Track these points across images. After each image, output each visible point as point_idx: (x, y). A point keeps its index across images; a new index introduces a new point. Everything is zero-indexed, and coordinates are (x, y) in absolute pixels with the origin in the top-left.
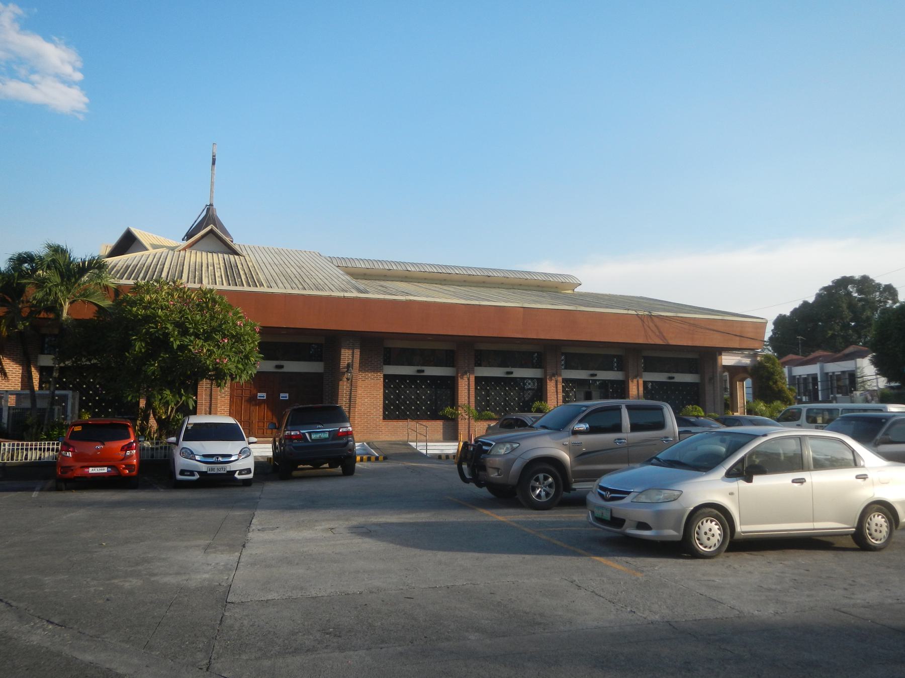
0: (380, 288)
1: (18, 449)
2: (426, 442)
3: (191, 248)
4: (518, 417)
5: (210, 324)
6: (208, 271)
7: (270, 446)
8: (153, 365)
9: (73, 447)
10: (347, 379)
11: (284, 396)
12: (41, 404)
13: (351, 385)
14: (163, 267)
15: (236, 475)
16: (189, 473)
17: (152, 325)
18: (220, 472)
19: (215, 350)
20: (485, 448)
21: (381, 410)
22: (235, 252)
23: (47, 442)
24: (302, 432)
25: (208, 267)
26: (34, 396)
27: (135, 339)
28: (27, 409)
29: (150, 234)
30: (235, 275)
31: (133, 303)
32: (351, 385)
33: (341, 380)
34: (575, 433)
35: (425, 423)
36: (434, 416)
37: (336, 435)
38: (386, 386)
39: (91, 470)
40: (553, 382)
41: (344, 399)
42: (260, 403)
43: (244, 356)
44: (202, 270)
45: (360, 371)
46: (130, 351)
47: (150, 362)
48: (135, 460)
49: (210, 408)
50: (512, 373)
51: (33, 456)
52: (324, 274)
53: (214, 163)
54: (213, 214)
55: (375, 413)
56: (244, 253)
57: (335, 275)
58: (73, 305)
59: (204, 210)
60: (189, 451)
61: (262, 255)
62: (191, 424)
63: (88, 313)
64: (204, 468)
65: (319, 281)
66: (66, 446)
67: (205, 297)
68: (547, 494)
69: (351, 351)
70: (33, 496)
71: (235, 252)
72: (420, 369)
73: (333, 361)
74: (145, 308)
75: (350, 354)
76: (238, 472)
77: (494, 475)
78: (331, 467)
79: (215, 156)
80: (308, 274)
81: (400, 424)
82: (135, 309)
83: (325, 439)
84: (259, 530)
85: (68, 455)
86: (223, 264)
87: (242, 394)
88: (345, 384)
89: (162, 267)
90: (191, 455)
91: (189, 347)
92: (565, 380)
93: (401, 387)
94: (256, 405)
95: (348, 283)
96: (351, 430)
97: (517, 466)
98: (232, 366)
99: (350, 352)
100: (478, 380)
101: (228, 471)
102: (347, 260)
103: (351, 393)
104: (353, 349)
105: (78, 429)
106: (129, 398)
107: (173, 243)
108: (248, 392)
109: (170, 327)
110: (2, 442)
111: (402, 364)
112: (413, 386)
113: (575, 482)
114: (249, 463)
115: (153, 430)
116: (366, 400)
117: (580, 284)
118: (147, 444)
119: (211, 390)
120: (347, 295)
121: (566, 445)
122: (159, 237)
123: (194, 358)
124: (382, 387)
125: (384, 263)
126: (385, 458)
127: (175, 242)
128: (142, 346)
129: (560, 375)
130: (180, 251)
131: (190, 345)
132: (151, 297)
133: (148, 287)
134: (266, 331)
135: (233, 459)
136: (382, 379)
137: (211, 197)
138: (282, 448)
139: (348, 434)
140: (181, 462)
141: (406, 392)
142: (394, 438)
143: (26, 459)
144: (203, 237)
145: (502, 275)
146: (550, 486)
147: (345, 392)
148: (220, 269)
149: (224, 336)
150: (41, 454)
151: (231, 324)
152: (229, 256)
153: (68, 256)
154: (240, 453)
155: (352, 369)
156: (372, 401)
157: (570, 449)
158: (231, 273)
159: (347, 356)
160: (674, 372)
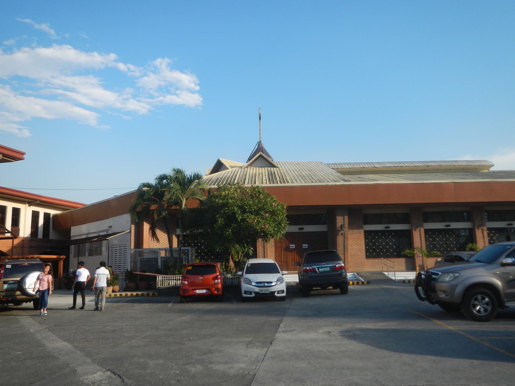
0: (358, 179)
1: (165, 279)
2: (394, 271)
3: (251, 166)
4: (457, 255)
5: (258, 205)
6: (259, 177)
7: (297, 275)
9: (188, 278)
10: (341, 234)
11: (305, 246)
12: (175, 255)
13: (344, 238)
14: (236, 177)
15: (276, 294)
16: (249, 293)
17: (227, 208)
18: (266, 292)
19: (261, 221)
20: (434, 276)
21: (364, 252)
22: (274, 166)
23: (178, 276)
24: (313, 267)
25: (259, 176)
27: (218, 217)
29: (230, 161)
30: (274, 178)
31: (216, 197)
32: (344, 238)
34: (504, 265)
35: (393, 260)
36: (399, 255)
37: (334, 269)
38: (366, 238)
39: (198, 291)
40: (479, 230)
41: (341, 246)
42: (292, 250)
43: (278, 223)
44: (256, 177)
45: (349, 229)
46: (217, 224)
47: (227, 229)
49: (264, 254)
50: (449, 226)
51: (172, 283)
52: (324, 173)
53: (260, 119)
54: (261, 146)
56: (279, 166)
57: (330, 173)
58: (188, 200)
59: (257, 145)
60: (248, 280)
61: (289, 166)
62: (249, 264)
63: (195, 205)
64: (257, 290)
65: (321, 177)
66: (184, 278)
68: (486, 310)
69: (343, 218)
70: (168, 306)
71: (274, 166)
73: (332, 223)
74: (222, 199)
75: (342, 219)
76: (276, 292)
77: (442, 296)
78: (334, 288)
79: (260, 115)
80: (315, 174)
81: (377, 261)
82: (217, 200)
83: (328, 272)
84: (283, 332)
85: (185, 283)
87: (281, 246)
88: (340, 237)
89: (235, 177)
90: (249, 282)
91: (247, 220)
92: (489, 229)
93: (376, 238)
95: (339, 177)
97: (459, 290)
99: (342, 218)
100: (427, 231)
101: (271, 292)
102: (338, 165)
104: (344, 216)
105: (190, 268)
106: (217, 250)
107: (241, 164)
109: (236, 209)
110: (157, 276)
111: (376, 224)
112: (383, 237)
113: (508, 301)
114: (282, 287)
115: (232, 268)
117: (493, 165)
118: (229, 276)
119: (264, 244)
120: (337, 183)
121: (497, 274)
122: (234, 162)
123: (250, 226)
124: (363, 238)
125: (360, 164)
126: (368, 283)
127: (242, 164)
128: (222, 220)
130: (245, 168)
131: (247, 219)
132: (226, 193)
133: (224, 187)
134: (290, 208)
135: (273, 284)
136: (363, 234)
137: (260, 137)
138: (302, 277)
139: (341, 268)
140: (245, 286)
141: (379, 241)
142: (373, 270)
143: (169, 285)
145: (437, 164)
146: (487, 304)
147: (340, 242)
148: (266, 175)
149: (267, 212)
150: (176, 282)
151: (269, 205)
153: (183, 174)
154: (277, 281)
155: (344, 228)
157: (500, 277)
158: (272, 177)
159: (341, 220)
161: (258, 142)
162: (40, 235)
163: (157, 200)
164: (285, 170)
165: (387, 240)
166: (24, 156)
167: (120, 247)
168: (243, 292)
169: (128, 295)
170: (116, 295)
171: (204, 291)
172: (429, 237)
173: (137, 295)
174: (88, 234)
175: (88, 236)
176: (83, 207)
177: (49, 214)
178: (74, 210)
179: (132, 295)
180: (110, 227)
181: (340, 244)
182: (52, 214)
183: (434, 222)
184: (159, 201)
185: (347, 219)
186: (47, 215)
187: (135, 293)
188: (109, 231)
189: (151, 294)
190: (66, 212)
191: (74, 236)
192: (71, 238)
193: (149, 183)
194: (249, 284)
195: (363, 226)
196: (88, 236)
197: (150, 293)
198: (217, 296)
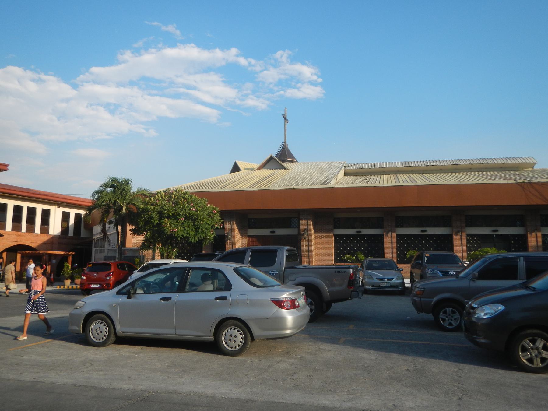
13: (308, 242)
32: (308, 242)
39: (93, 286)
40: (458, 236)
50: (425, 231)
69: (306, 221)
72: (494, 229)
75: (306, 223)
92: (468, 235)
99: (306, 221)
103: (309, 247)
104: (307, 220)
119: (232, 246)
129: (465, 232)
156: (326, 251)
160: (498, 227)
162: (71, 233)
166: (8, 167)
170: (77, 287)
177: (81, 215)
186: (77, 216)
195: (333, 231)
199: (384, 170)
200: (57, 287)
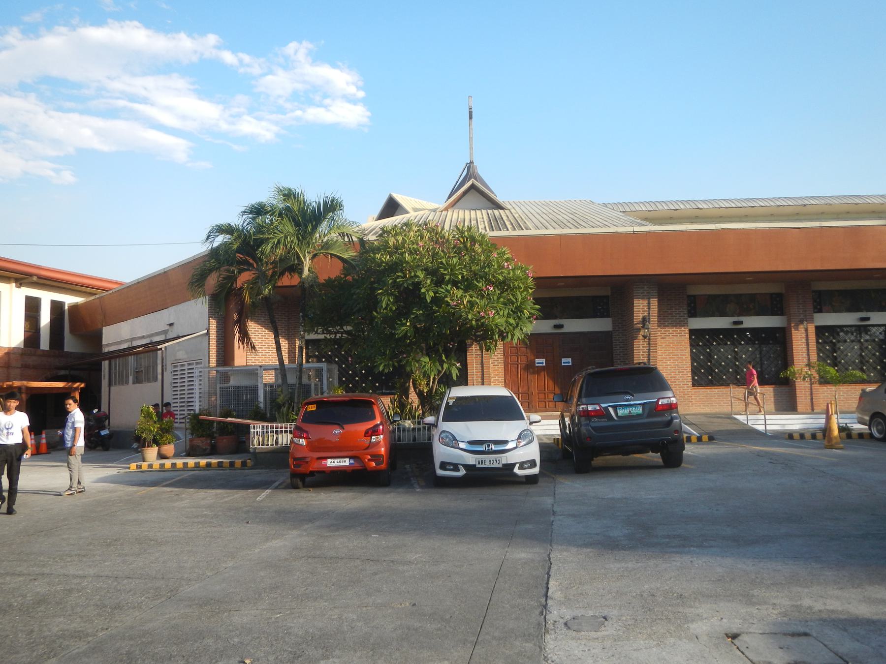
1: (267, 432)
3: (454, 207)
5: (471, 268)
7: (557, 422)
8: (405, 324)
9: (307, 432)
10: (643, 336)
11: (567, 361)
12: (292, 379)
13: (649, 344)
15: (516, 470)
16: (452, 467)
17: (400, 274)
18: (492, 466)
19: (478, 301)
21: (689, 374)
24: (603, 405)
25: (471, 222)
26: (285, 369)
27: (381, 294)
28: (279, 386)
29: (412, 199)
30: (500, 226)
31: (377, 250)
32: (649, 344)
33: (636, 338)
37: (654, 410)
39: (330, 463)
43: (516, 308)
46: (378, 310)
47: (401, 321)
48: (383, 449)
49: (483, 379)
50: (868, 319)
53: (471, 117)
54: (474, 172)
55: (681, 379)
56: (509, 207)
58: (315, 260)
60: (450, 436)
61: (528, 208)
62: (452, 398)
63: (333, 271)
64: (471, 459)
66: (298, 432)
67: (462, 237)
69: (647, 302)
70: (258, 499)
71: (499, 207)
76: (517, 466)
82: (378, 256)
85: (301, 443)
86: (487, 218)
88: (641, 343)
90: (452, 441)
91: (446, 299)
94: (533, 373)
96: (675, 402)
98: (500, 321)
99: (646, 302)
101: (503, 465)
103: (649, 355)
104: (649, 299)
105: (312, 408)
106: (381, 368)
107: (434, 206)
108: (524, 358)
109: (421, 274)
111: (713, 315)
112: (729, 343)
114: (532, 452)
115: (414, 407)
116: (668, 362)
118: (408, 424)
119: (482, 357)
123: (454, 313)
124: (688, 345)
125: (668, 203)
126: (711, 439)
128: (390, 301)
130: (442, 211)
132: (397, 241)
133: (396, 231)
135: (510, 446)
136: (687, 336)
137: (471, 154)
139: (672, 407)
140: (441, 452)
141: (720, 351)
142: (707, 410)
143: (277, 443)
144: (465, 193)
145: (823, 202)
147: (641, 353)
148: (484, 222)
152: (493, 211)
154: (519, 437)
155: (650, 323)
156: (677, 363)
161: (467, 164)
162: (45, 344)
163: (251, 261)
164: (522, 214)
165: (736, 350)
167: (189, 364)
168: (437, 465)
169: (189, 466)
171: (345, 461)
172: (825, 342)
173: (209, 465)
174: (132, 339)
175: (132, 343)
176: (124, 286)
178: (104, 294)
179: (197, 465)
180: (171, 325)
181: (641, 356)
182: (68, 304)
183: (835, 311)
184: (255, 265)
185: (657, 304)
186: (57, 308)
187: (203, 462)
188: (170, 333)
189: (238, 462)
190: (92, 298)
191: (108, 345)
192: (103, 349)
193: (232, 224)
194: (452, 447)
195: (688, 321)
196: (132, 343)
197: (236, 461)
198: (376, 473)
199: (698, 212)
200: (129, 468)
